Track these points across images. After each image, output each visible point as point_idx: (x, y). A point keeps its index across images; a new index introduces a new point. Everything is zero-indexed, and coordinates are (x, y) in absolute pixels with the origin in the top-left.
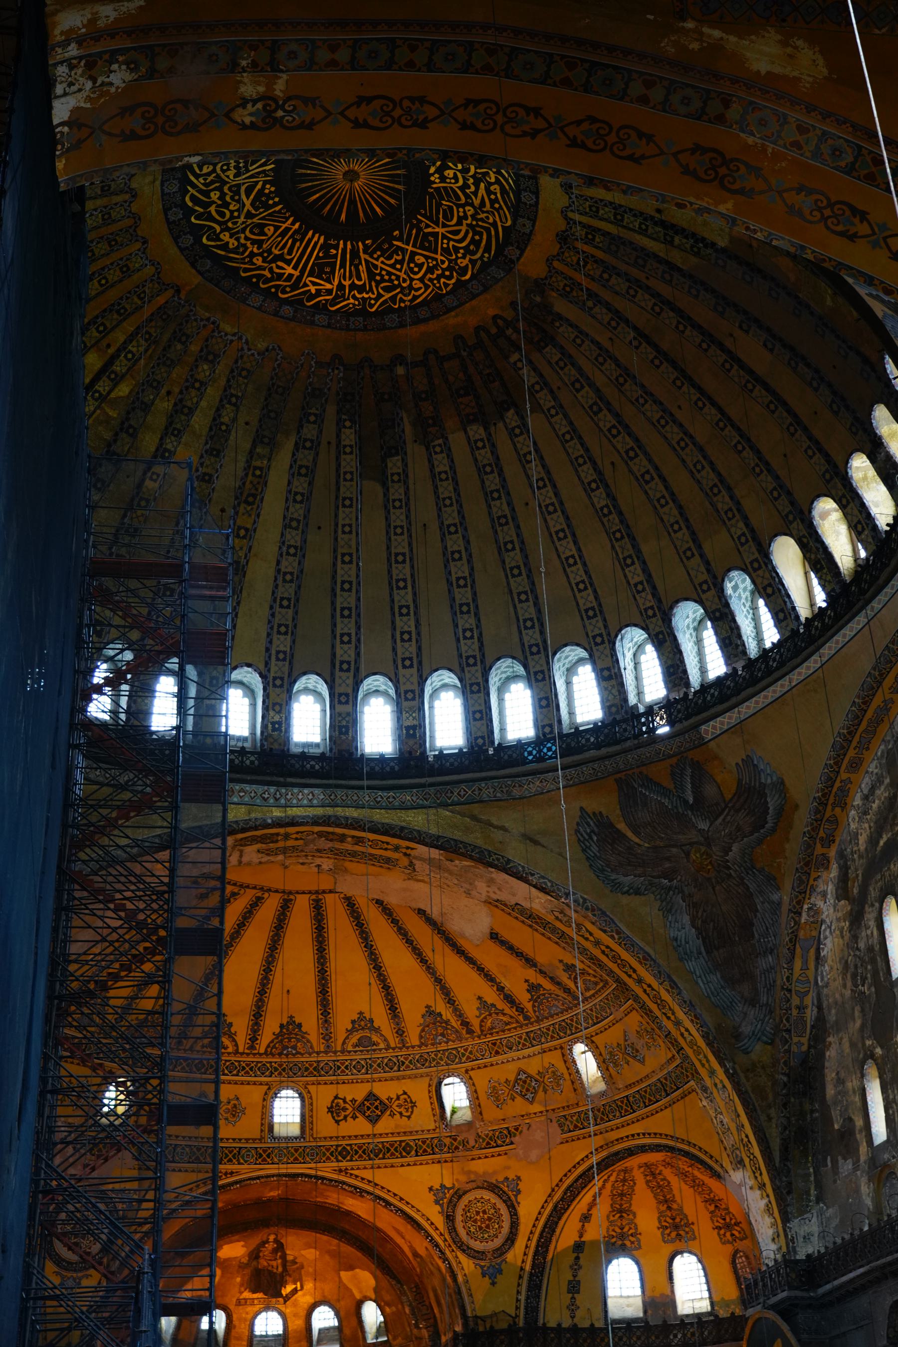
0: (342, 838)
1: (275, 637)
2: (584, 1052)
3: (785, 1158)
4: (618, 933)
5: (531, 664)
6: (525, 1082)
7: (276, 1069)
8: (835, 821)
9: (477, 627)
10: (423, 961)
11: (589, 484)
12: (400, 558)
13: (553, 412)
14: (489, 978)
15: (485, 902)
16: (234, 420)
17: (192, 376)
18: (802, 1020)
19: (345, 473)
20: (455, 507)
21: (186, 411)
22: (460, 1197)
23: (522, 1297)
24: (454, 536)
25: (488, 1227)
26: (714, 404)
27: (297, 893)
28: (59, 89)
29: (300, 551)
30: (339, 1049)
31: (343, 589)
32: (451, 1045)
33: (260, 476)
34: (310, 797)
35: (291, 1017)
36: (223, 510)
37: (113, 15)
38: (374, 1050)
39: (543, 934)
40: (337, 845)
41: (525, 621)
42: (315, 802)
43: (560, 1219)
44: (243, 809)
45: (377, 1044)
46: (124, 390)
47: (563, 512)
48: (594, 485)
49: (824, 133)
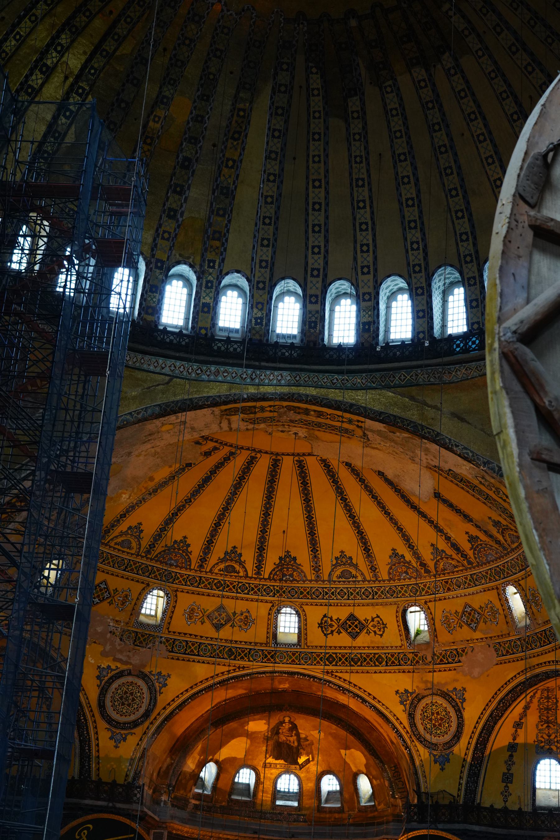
0: (307, 412)
2: (515, 593)
5: (465, 271)
6: (470, 614)
7: (253, 589)
9: (423, 240)
10: (387, 513)
11: (512, 115)
13: (480, 53)
17: (182, 35)
19: (314, 112)
20: (404, 139)
21: (179, 63)
22: (419, 700)
23: (464, 782)
24: (404, 164)
25: (440, 725)
27: (283, 454)
30: (326, 578)
31: (314, 209)
32: (413, 581)
33: (243, 117)
34: (279, 378)
35: (288, 552)
36: (214, 145)
38: (354, 582)
39: (473, 496)
40: (304, 417)
41: (461, 234)
42: (283, 382)
43: (495, 723)
44: (225, 386)
45: (356, 577)
46: (126, 48)
47: (491, 141)
48: (515, 117)
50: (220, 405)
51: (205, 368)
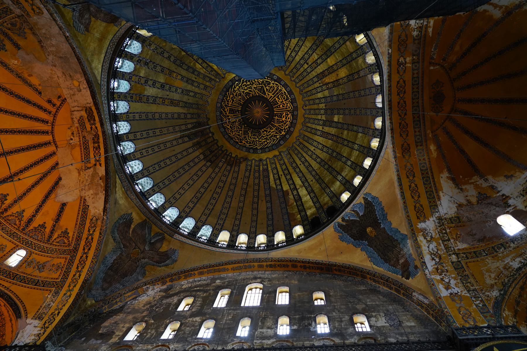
1: (138, 114)
3: (69, 325)
4: (103, 238)
8: (179, 278)
10: (33, 186)
12: (165, 146)
14: (37, 211)
15: (81, 196)
16: (190, 96)
18: (113, 305)
20: (181, 157)
26: (244, 204)
27: (53, 135)
28: (418, 21)
29: (161, 118)
31: (153, 132)
36: (168, 95)
37: (430, 31)
49: (426, 163)
50: (95, 106)
51: (105, 98)
